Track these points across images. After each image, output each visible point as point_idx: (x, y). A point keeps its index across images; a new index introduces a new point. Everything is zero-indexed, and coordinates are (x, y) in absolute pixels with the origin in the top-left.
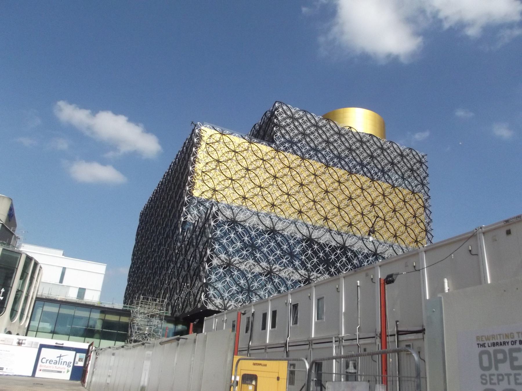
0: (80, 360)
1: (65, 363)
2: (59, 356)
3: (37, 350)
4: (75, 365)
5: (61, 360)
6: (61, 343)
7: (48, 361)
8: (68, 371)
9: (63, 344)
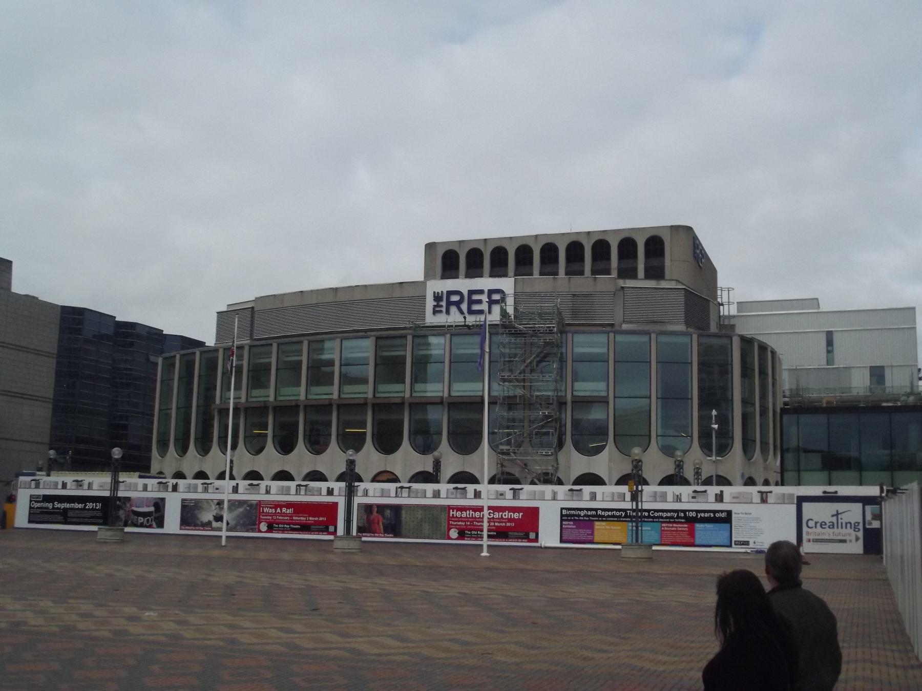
1: (849, 525)
2: (836, 513)
3: (793, 508)
4: (868, 527)
5: (840, 521)
6: (833, 491)
7: (818, 525)
8: (857, 539)
9: (836, 492)
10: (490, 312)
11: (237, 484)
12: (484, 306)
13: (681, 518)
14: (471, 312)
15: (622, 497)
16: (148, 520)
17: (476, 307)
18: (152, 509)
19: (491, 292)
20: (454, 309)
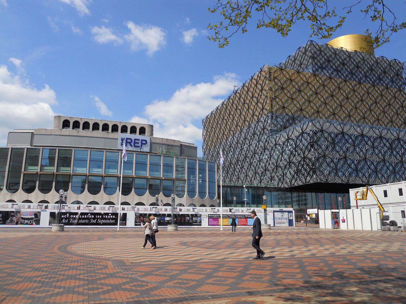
0: (291, 216)
8: (287, 222)
10: (141, 147)
11: (80, 206)
12: (140, 144)
13: (244, 217)
14: (135, 146)
15: (227, 211)
16: (30, 222)
17: (136, 145)
18: (33, 216)
19: (142, 140)
20: (128, 144)
